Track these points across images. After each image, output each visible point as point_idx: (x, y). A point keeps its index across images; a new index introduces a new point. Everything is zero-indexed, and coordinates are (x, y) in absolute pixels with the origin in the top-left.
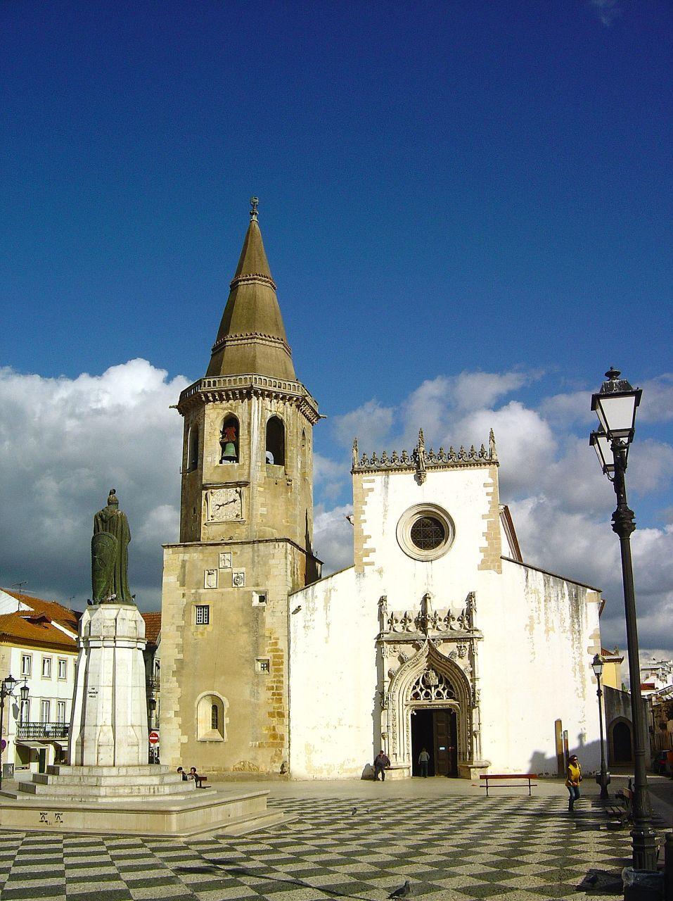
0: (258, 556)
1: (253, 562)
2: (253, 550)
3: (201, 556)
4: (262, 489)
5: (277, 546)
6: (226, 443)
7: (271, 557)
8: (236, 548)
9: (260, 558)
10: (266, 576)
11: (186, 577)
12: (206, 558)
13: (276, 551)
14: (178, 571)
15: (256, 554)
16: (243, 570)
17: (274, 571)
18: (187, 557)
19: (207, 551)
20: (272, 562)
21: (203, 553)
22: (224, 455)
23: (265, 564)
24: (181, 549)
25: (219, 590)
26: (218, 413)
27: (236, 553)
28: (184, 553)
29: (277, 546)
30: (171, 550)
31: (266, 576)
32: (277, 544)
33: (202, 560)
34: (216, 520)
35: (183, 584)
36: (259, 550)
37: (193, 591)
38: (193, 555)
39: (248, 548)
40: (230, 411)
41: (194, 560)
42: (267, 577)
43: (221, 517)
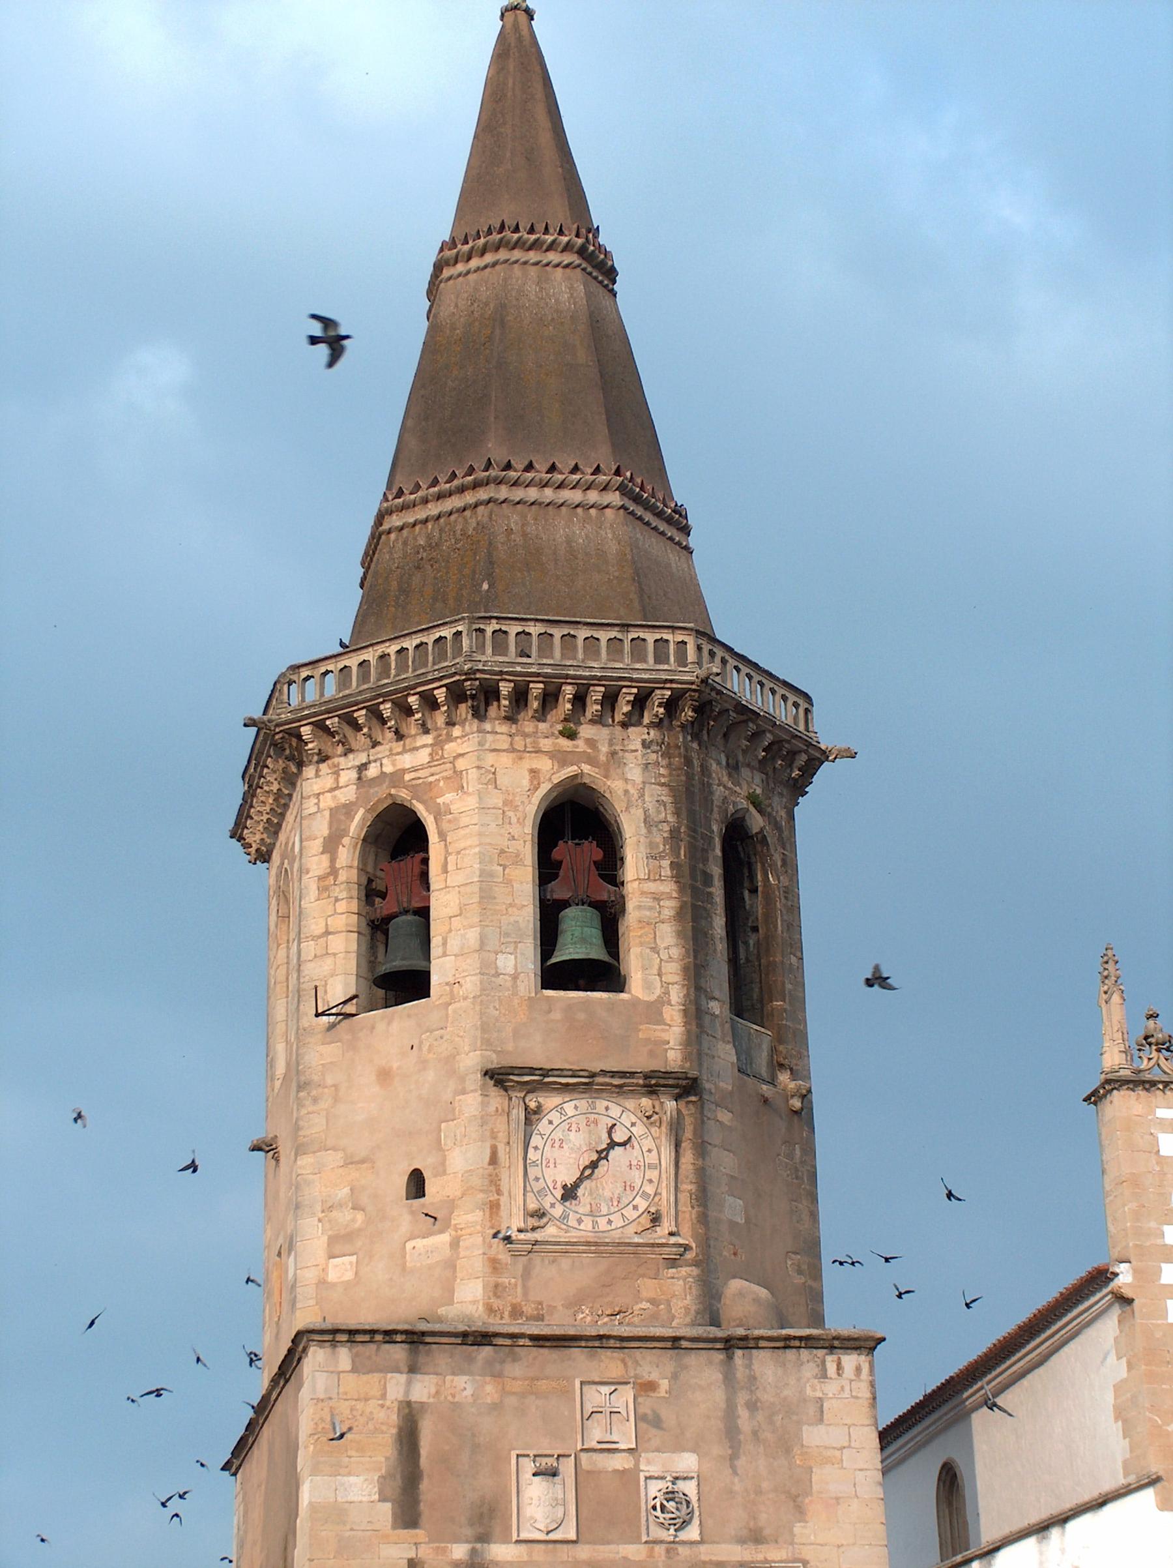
0: (752, 1406)
1: (731, 1432)
2: (729, 1378)
3: (490, 1390)
4: (725, 1117)
5: (831, 1368)
6: (565, 904)
7: (812, 1410)
8: (652, 1366)
9: (760, 1416)
10: (794, 1498)
11: (424, 1485)
12: (511, 1401)
13: (831, 1388)
14: (382, 1452)
15: (742, 1398)
16: (688, 1462)
17: (826, 1480)
18: (422, 1389)
19: (515, 1370)
20: (814, 1436)
21: (498, 1375)
22: (569, 950)
23: (786, 1444)
24: (398, 1352)
25: (583, 1552)
26: (534, 772)
27: (648, 1387)
28: (413, 1369)
29: (831, 1368)
30: (344, 1356)
31: (794, 1498)
32: (831, 1362)
33: (497, 1407)
34: (551, 1232)
35: (408, 1514)
36: (753, 1379)
37: (460, 1551)
38: (452, 1388)
39: (704, 1370)
40: (586, 768)
41: (456, 1406)
42: (796, 1498)
43: (572, 1222)
